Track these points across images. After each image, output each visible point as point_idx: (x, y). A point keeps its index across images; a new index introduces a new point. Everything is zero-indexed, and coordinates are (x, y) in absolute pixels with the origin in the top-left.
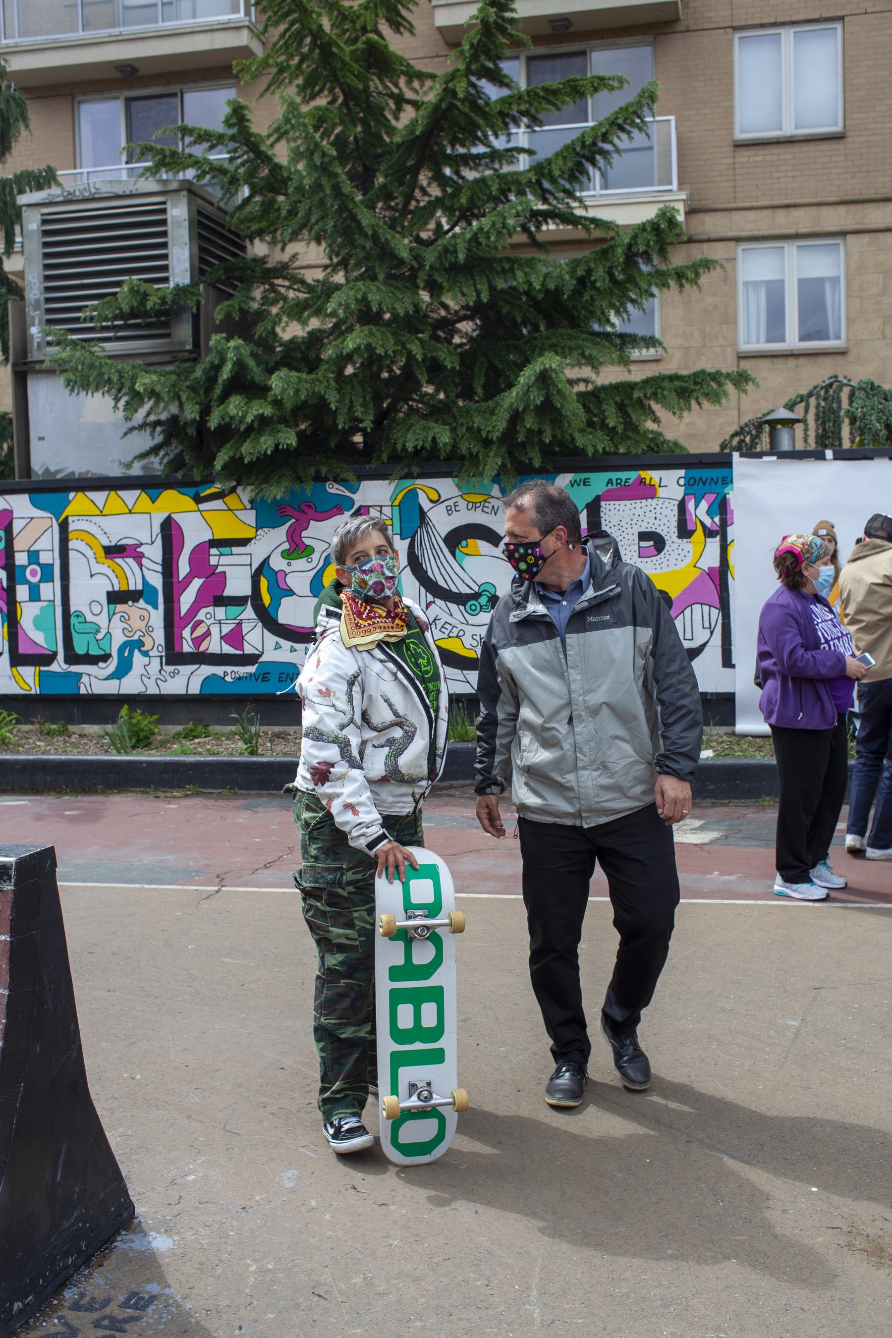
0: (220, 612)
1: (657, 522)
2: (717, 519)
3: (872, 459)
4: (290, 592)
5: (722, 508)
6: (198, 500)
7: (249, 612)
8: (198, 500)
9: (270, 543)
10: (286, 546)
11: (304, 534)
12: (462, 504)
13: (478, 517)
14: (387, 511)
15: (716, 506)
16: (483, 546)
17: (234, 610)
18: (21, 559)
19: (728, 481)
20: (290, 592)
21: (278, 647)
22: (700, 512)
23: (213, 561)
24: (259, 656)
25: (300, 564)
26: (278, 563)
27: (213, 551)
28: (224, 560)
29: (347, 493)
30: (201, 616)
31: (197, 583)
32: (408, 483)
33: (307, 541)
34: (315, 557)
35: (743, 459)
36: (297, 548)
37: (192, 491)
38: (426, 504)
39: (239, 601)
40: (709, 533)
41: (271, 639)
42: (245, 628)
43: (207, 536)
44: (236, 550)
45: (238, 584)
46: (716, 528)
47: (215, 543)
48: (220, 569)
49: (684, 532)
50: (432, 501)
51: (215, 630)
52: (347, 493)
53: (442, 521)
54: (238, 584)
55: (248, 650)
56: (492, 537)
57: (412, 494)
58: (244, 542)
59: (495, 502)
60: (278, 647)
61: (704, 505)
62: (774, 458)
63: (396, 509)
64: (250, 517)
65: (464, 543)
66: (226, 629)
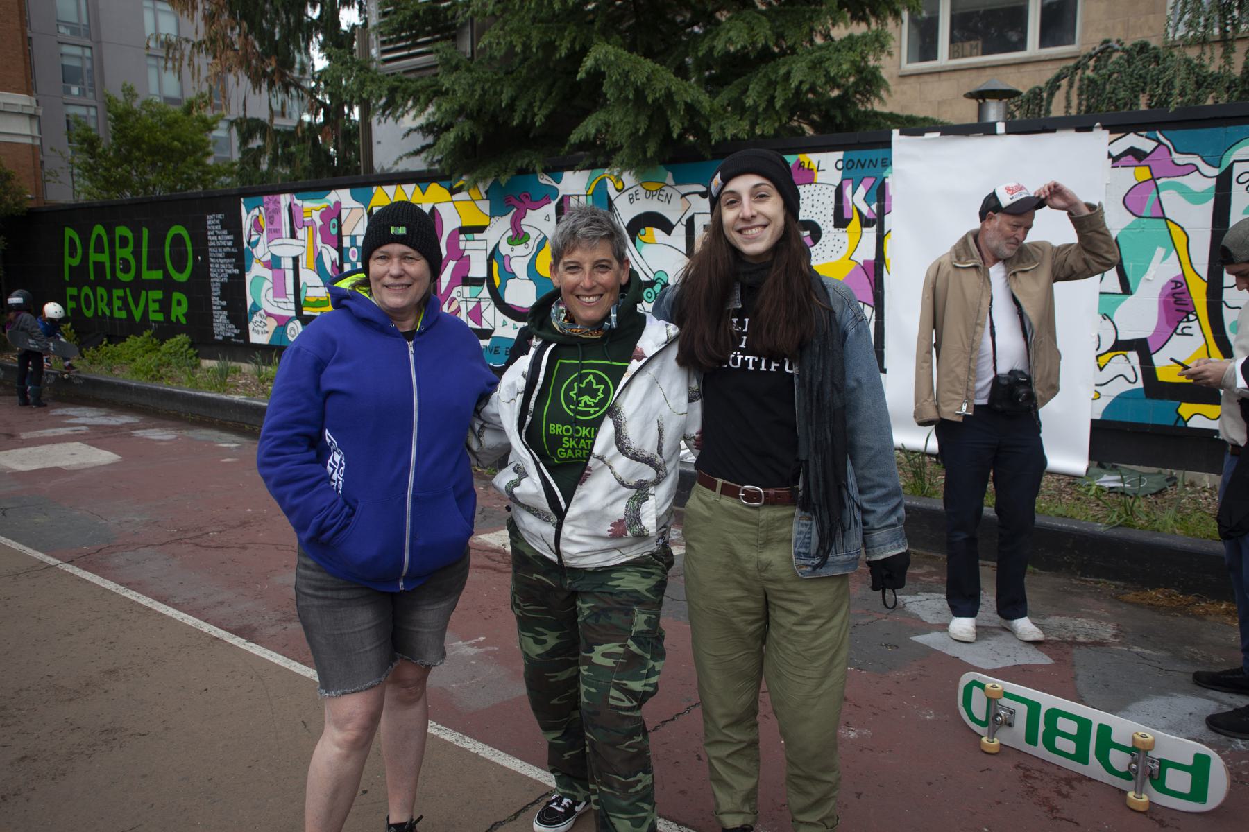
0: (466, 291)
1: (814, 210)
2: (874, 207)
3: (1054, 131)
4: (513, 275)
5: (880, 194)
6: (453, 192)
7: (485, 292)
8: (453, 192)
9: (500, 228)
10: (510, 233)
11: (523, 222)
12: (642, 192)
13: (654, 206)
14: (583, 199)
15: (874, 191)
16: (658, 234)
17: (476, 289)
18: (346, 242)
19: (887, 163)
20: (513, 275)
21: (505, 325)
22: (857, 199)
23: (462, 245)
24: (492, 331)
25: (520, 249)
26: (505, 249)
27: (462, 237)
28: (470, 245)
29: (554, 184)
30: (454, 294)
31: (452, 264)
32: (599, 173)
33: (525, 229)
34: (531, 243)
35: (904, 138)
36: (518, 236)
37: (447, 184)
38: (613, 193)
39: (477, 282)
40: (866, 222)
41: (501, 317)
42: (484, 305)
43: (458, 225)
44: (477, 236)
45: (478, 269)
46: (872, 216)
47: (464, 230)
48: (466, 253)
49: (841, 221)
50: (618, 190)
51: (463, 306)
52: (554, 184)
53: (626, 211)
54: (478, 269)
55: (485, 326)
56: (667, 227)
57: (602, 184)
58: (481, 229)
59: (668, 190)
60: (505, 325)
61: (862, 191)
62: (937, 134)
63: (590, 198)
64: (485, 206)
65: (642, 231)
66: (471, 306)
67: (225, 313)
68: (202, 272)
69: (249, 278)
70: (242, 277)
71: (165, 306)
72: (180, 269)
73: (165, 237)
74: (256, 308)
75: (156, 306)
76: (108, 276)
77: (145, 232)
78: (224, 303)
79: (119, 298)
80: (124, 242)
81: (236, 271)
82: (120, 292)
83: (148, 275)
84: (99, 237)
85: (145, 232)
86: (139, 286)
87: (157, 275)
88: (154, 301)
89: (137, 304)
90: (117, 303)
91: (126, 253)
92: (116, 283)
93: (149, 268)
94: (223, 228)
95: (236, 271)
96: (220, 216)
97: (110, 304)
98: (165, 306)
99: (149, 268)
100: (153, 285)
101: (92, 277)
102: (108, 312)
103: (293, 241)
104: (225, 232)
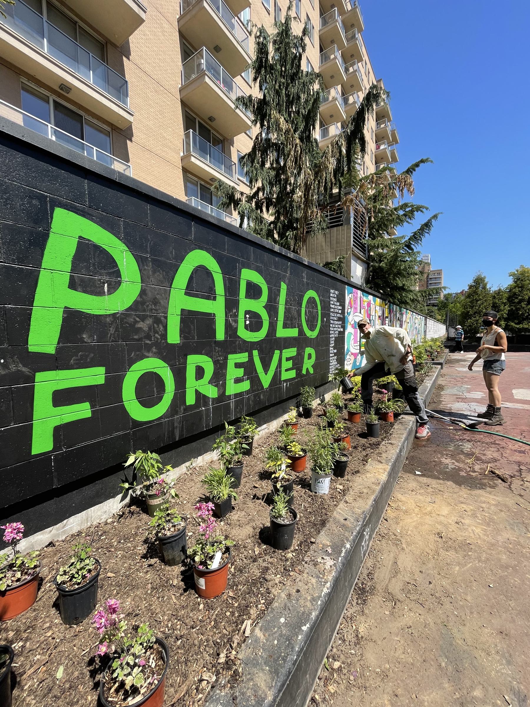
67: (336, 357)
68: (325, 330)
69: (346, 333)
70: (343, 333)
71: (297, 363)
72: (312, 328)
73: (303, 296)
74: (348, 350)
75: (290, 364)
76: (220, 335)
77: (284, 287)
78: (335, 351)
79: (238, 365)
80: (253, 291)
81: (342, 330)
82: (243, 357)
83: (282, 332)
84: (201, 275)
85: (284, 287)
86: (269, 346)
87: (293, 333)
88: (288, 359)
89: (266, 367)
90: (233, 372)
91: (258, 306)
92: (233, 343)
93: (285, 326)
94: (338, 301)
95: (342, 330)
96: (337, 292)
97: (218, 379)
98: (297, 363)
99: (285, 326)
100: (287, 343)
101: (174, 336)
102: (212, 392)
103: (360, 315)
104: (338, 304)
